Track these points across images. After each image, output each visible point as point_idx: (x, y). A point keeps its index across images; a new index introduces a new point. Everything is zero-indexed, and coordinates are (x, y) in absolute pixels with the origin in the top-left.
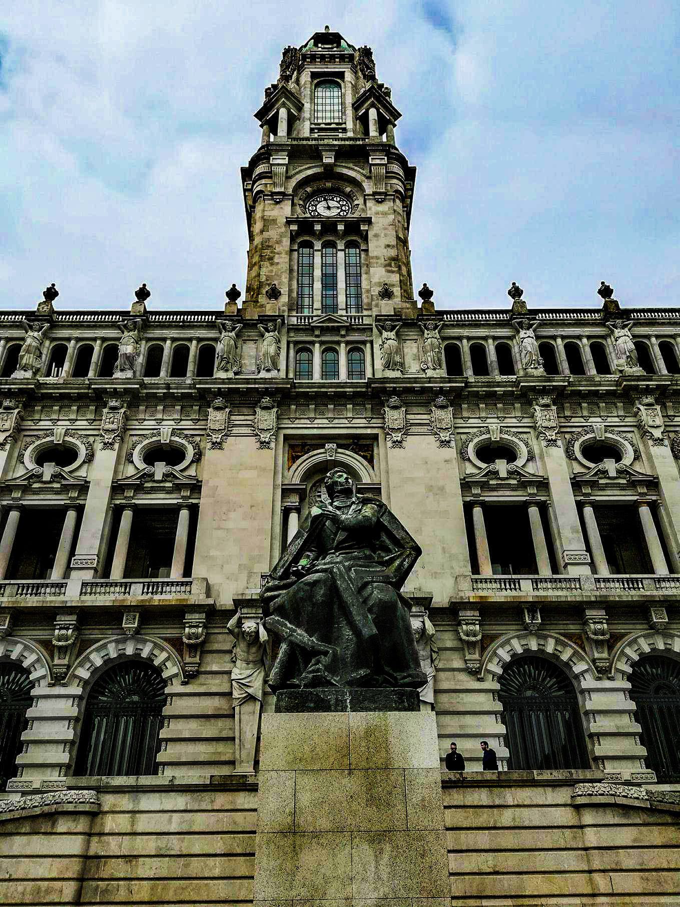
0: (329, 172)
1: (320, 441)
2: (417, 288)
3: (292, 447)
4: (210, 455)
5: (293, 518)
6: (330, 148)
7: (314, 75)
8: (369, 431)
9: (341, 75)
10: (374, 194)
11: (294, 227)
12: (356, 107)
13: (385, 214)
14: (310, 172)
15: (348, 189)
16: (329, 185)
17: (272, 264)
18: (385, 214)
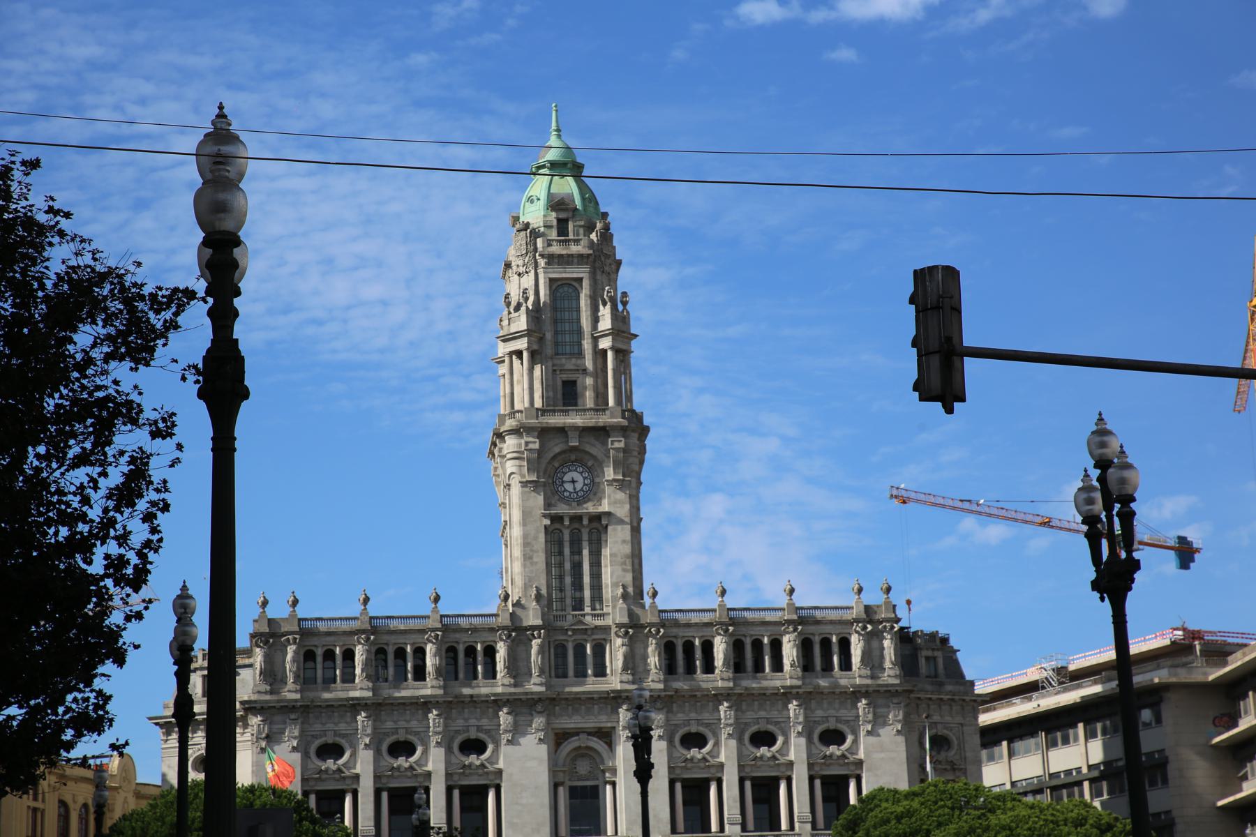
0: (573, 449)
1: (577, 733)
2: (647, 587)
3: (556, 734)
4: (504, 749)
5: (561, 789)
6: (575, 428)
7: (551, 280)
8: (609, 725)
9: (580, 280)
10: (615, 480)
11: (547, 522)
12: (595, 340)
13: (621, 502)
14: (557, 450)
15: (590, 464)
16: (573, 457)
17: (532, 564)
18: (621, 502)
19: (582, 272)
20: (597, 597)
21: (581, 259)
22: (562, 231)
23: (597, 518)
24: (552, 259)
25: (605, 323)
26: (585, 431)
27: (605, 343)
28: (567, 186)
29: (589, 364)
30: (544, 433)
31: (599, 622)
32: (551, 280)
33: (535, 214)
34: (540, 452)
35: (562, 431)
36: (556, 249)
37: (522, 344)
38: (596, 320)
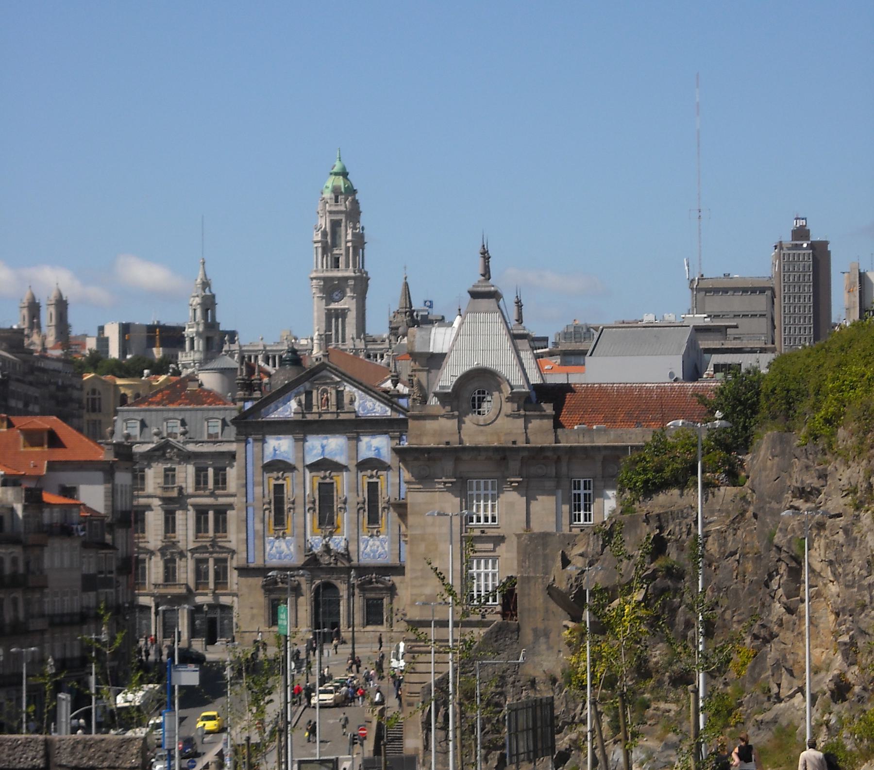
19: (342, 217)
20: (344, 341)
21: (340, 212)
22: (337, 201)
23: (344, 310)
24: (331, 212)
25: (349, 238)
26: (339, 279)
27: (349, 244)
28: (340, 182)
29: (343, 252)
30: (325, 279)
31: (344, 347)
32: (331, 220)
33: (328, 195)
34: (324, 285)
35: (332, 279)
36: (334, 209)
37: (320, 245)
38: (346, 235)
